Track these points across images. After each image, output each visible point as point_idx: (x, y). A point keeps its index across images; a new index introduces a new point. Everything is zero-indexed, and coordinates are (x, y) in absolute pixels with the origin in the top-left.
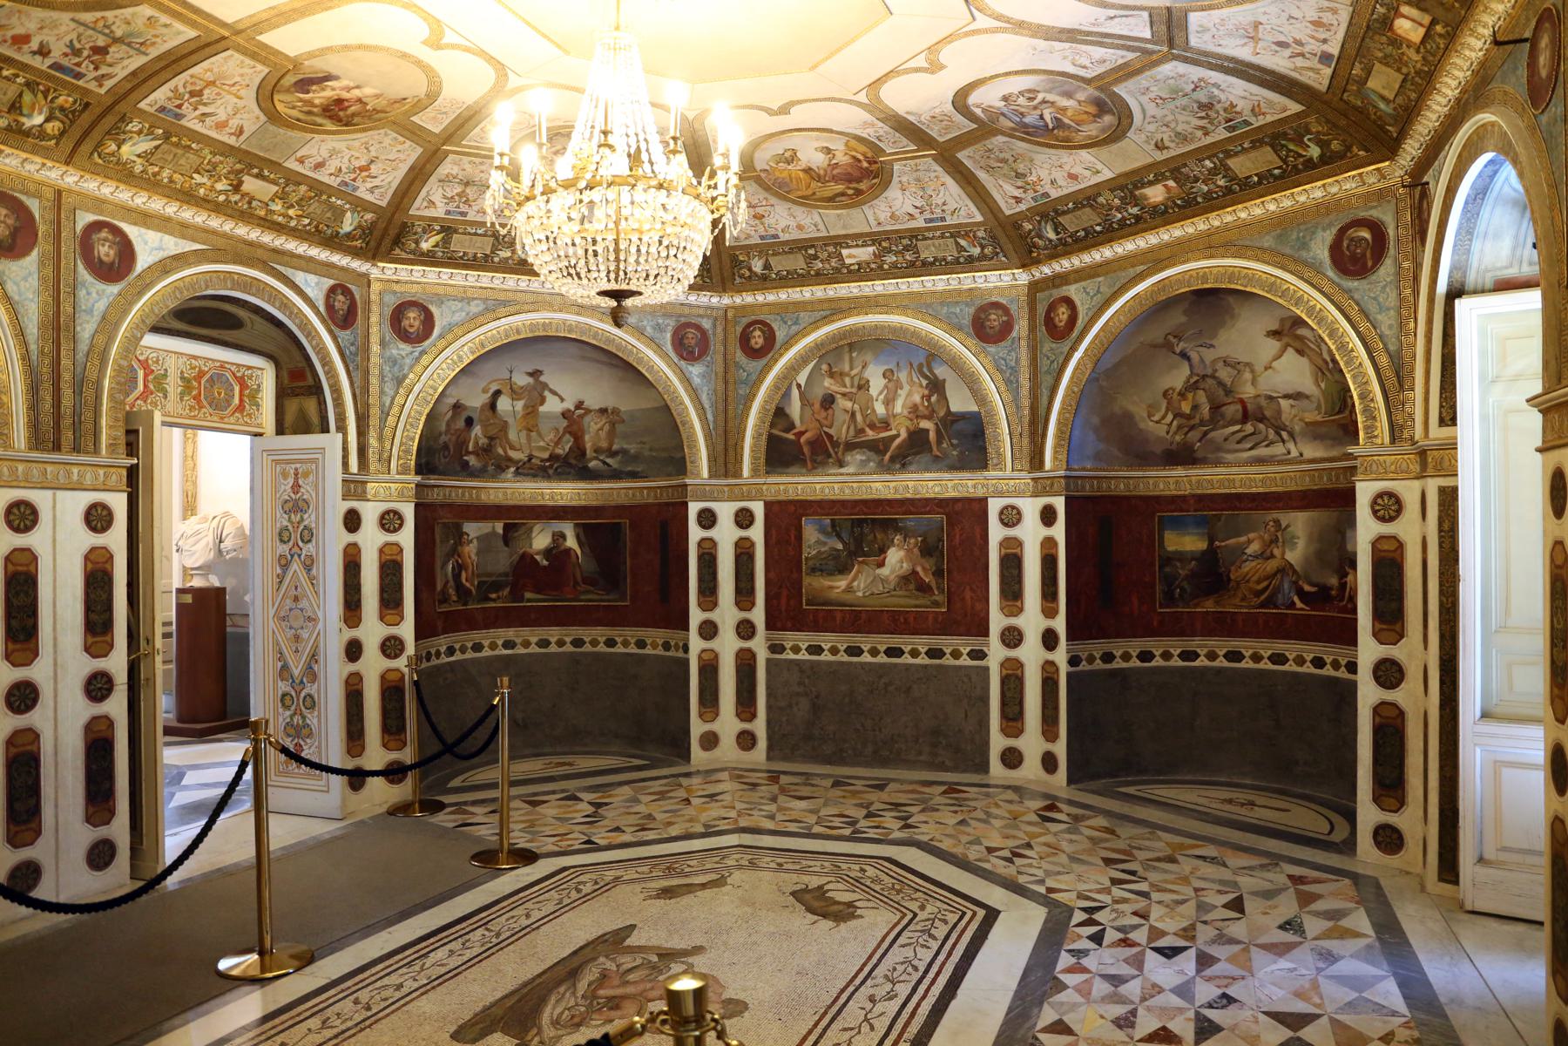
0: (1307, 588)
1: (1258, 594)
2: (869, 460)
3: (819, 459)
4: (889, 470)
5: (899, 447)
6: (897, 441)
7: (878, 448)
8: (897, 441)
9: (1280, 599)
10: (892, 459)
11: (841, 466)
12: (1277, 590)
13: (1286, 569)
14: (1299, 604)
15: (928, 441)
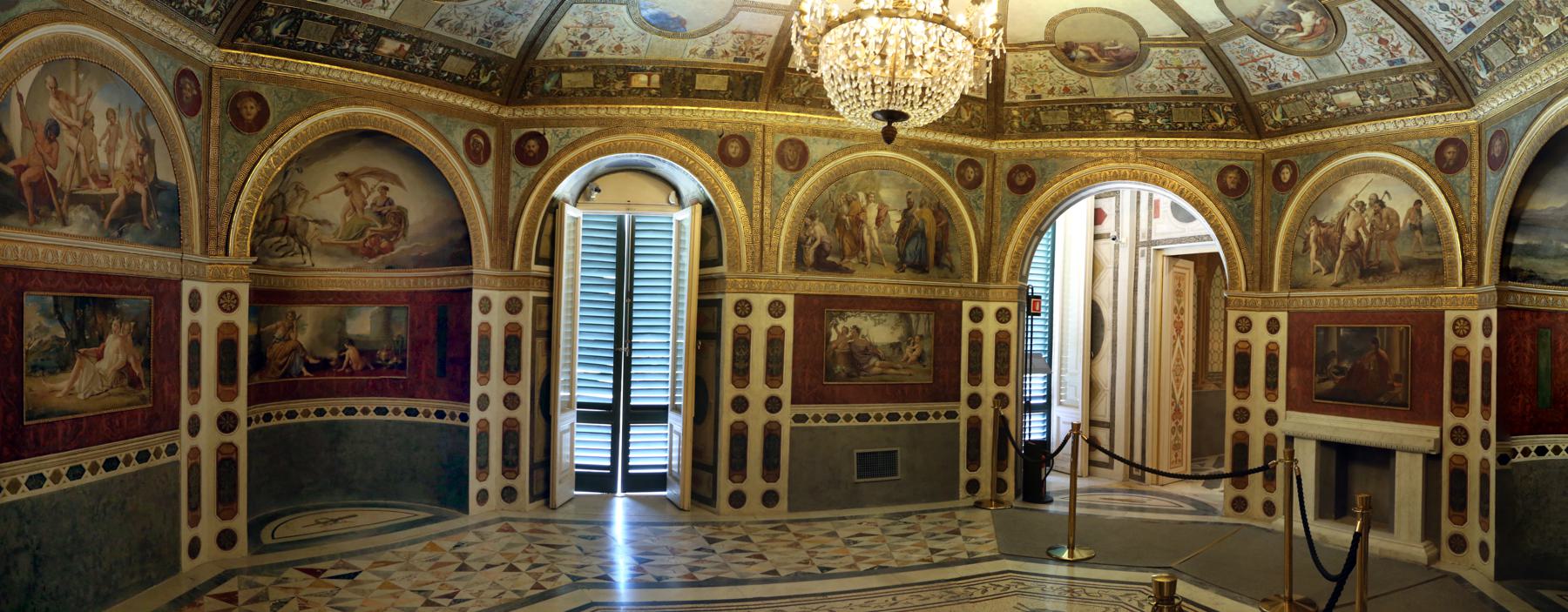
0: (312, 361)
1: (281, 367)
2: (91, 221)
3: (42, 210)
4: (110, 239)
5: (118, 210)
6: (116, 203)
7: (98, 205)
8: (116, 203)
9: (293, 371)
10: (112, 222)
11: (65, 224)
12: (292, 363)
13: (298, 348)
14: (306, 373)
15: (140, 209)
